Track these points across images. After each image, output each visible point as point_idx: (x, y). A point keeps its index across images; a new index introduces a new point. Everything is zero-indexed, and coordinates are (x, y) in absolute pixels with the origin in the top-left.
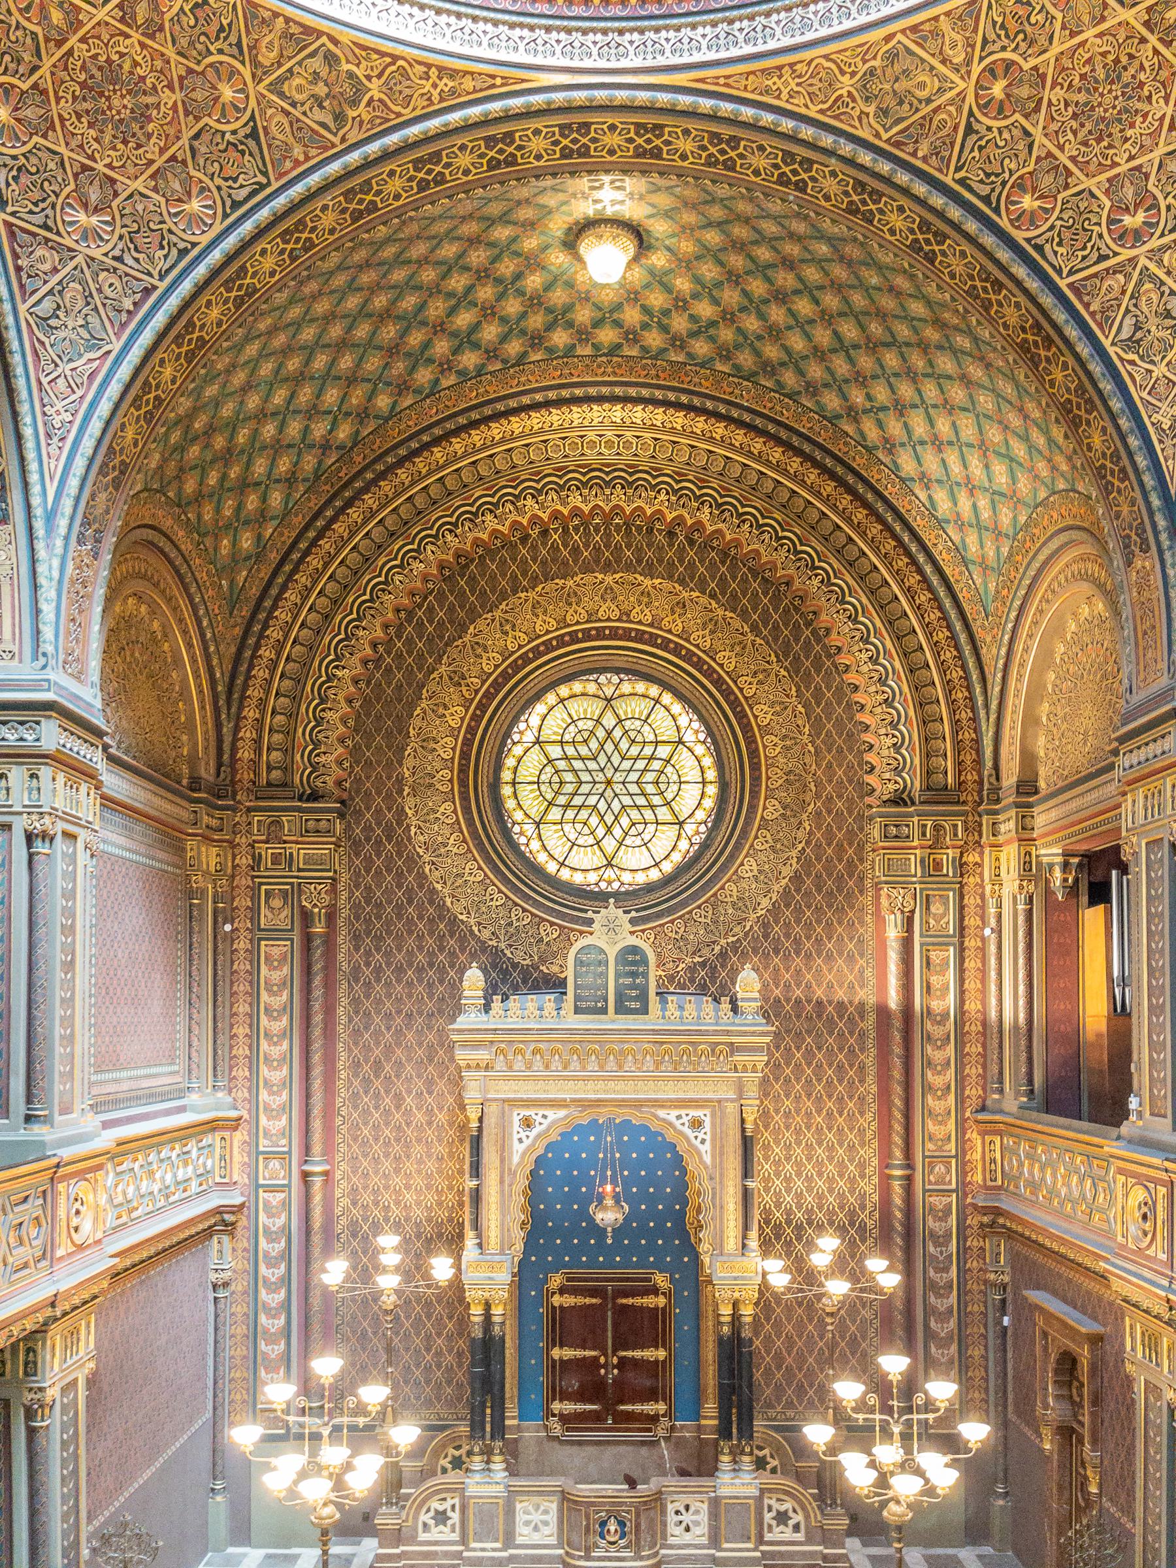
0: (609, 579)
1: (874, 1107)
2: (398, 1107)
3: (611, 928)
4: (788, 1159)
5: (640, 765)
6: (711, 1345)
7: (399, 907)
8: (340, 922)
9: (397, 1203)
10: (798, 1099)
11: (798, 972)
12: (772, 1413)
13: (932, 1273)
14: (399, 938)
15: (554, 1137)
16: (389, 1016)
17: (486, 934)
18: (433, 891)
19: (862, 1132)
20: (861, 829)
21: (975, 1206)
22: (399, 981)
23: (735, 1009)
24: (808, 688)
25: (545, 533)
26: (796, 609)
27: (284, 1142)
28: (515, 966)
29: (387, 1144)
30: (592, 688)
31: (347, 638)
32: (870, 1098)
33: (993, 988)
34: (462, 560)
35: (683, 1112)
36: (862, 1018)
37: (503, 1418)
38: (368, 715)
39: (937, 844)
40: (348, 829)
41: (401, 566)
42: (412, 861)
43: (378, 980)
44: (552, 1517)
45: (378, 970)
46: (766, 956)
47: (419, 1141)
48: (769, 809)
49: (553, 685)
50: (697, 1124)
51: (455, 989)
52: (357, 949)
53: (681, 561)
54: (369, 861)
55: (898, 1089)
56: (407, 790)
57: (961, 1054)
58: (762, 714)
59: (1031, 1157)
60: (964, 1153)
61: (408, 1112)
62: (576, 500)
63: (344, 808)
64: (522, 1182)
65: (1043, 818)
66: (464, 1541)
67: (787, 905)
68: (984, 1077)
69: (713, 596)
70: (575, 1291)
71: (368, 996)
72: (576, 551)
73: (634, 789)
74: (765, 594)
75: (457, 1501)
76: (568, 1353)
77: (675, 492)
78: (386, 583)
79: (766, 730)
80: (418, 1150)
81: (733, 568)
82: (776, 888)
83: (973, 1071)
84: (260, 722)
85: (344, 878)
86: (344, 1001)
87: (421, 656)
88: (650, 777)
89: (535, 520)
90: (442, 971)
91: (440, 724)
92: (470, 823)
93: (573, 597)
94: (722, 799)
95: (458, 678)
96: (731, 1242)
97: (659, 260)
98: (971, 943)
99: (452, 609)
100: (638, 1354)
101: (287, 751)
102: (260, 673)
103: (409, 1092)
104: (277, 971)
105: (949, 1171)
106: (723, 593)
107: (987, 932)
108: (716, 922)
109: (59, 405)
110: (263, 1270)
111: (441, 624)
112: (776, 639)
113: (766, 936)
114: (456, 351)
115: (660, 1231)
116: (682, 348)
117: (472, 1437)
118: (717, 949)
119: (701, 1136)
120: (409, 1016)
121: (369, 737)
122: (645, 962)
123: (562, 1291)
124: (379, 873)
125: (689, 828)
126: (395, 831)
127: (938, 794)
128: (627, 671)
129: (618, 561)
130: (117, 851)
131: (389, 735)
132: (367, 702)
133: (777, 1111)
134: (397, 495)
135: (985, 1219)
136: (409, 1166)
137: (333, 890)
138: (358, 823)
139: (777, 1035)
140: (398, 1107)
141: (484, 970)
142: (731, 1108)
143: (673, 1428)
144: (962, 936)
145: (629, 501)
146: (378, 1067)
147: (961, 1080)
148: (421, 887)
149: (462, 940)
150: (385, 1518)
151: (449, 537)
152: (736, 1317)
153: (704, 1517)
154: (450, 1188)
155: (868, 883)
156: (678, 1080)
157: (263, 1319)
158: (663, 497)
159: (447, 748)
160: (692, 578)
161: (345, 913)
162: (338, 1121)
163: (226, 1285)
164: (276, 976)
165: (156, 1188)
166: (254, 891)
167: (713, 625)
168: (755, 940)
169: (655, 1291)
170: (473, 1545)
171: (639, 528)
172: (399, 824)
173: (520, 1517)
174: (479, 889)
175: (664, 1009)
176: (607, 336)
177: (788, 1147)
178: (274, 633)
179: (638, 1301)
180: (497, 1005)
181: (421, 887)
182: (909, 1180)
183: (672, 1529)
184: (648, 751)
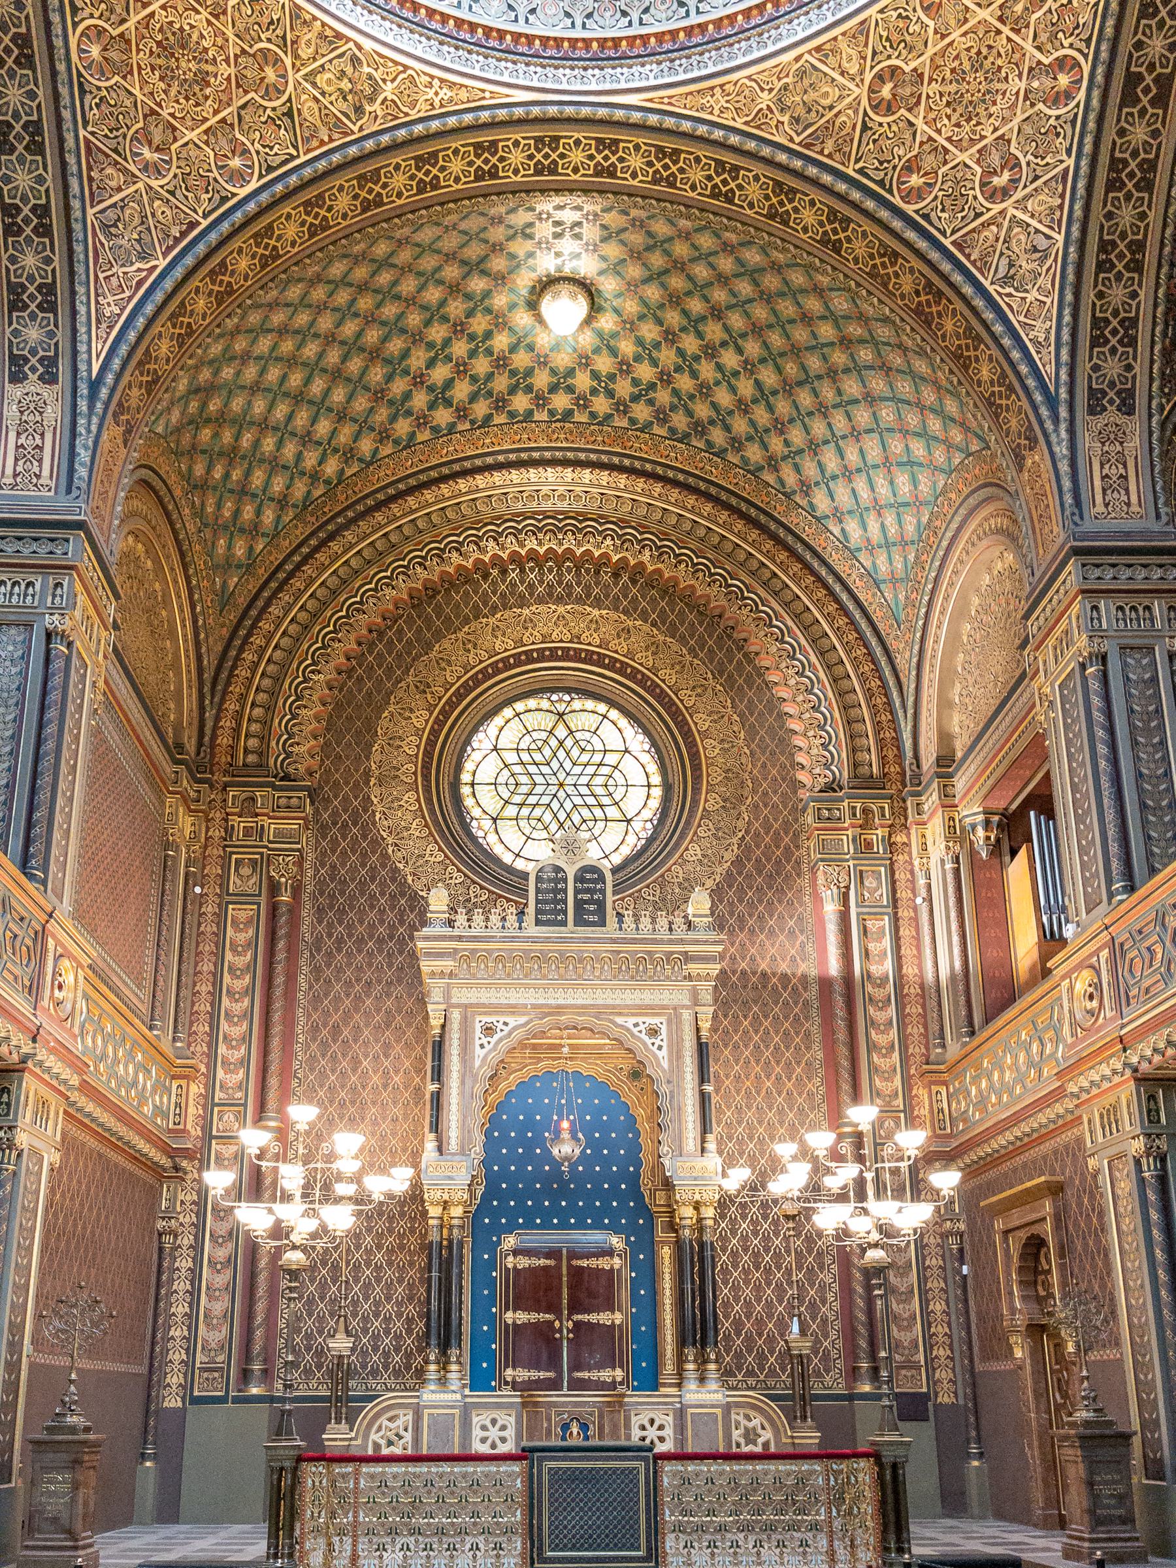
0: (561, 609)
1: (821, 1072)
2: (354, 1070)
5: (590, 770)
8: (305, 897)
11: (742, 945)
14: (362, 912)
16: (348, 984)
22: (360, 951)
25: (504, 572)
26: (730, 637)
30: (545, 704)
33: (928, 952)
35: (640, 1020)
39: (866, 825)
40: (317, 812)
42: (377, 843)
43: (339, 950)
45: (340, 941)
47: (374, 1103)
48: (710, 801)
49: (509, 702)
50: (653, 1032)
54: (335, 843)
55: (843, 1051)
58: (700, 722)
60: (912, 1109)
61: (365, 1074)
63: (313, 793)
65: (960, 783)
67: (730, 886)
68: (926, 1036)
69: (654, 624)
71: (328, 965)
72: (531, 586)
73: (584, 790)
79: (705, 735)
81: (672, 603)
83: (915, 1030)
84: (238, 716)
85: (311, 857)
87: (390, 669)
91: (406, 729)
92: (432, 811)
95: (423, 687)
97: (607, 322)
98: (904, 913)
101: (264, 738)
102: (242, 672)
104: (242, 932)
107: (919, 901)
111: (409, 642)
116: (625, 412)
120: (369, 984)
124: (344, 853)
125: (637, 825)
126: (361, 816)
127: (864, 782)
128: (577, 691)
129: (569, 595)
131: (358, 733)
132: (339, 706)
140: (354, 1070)
144: (895, 907)
146: (336, 1031)
148: (384, 866)
155: (805, 867)
159: (412, 746)
161: (310, 888)
162: (294, 1083)
164: (242, 938)
166: (225, 861)
167: (655, 648)
171: (588, 571)
172: (365, 811)
177: (739, 1110)
178: (257, 640)
181: (384, 866)
184: (597, 758)
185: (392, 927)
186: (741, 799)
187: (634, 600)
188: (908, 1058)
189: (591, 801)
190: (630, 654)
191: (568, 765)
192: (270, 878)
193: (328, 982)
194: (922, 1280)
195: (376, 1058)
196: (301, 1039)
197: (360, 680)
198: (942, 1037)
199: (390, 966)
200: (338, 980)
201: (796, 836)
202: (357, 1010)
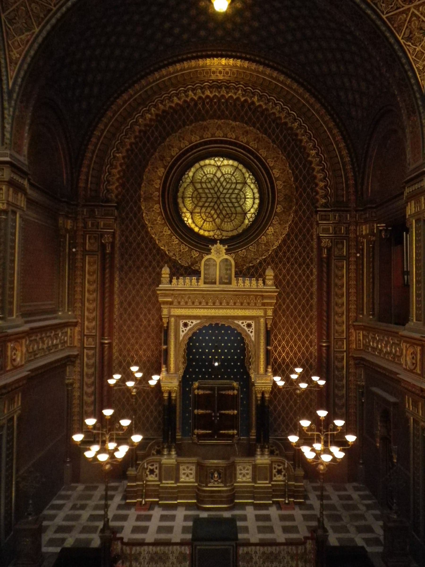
0: (219, 122)
3: (218, 252)
4: (284, 339)
6: (254, 409)
7: (139, 245)
8: (116, 249)
9: (137, 355)
10: (288, 317)
12: (276, 434)
13: (336, 382)
15: (195, 330)
16: (134, 285)
17: (171, 254)
18: (152, 238)
19: (311, 329)
20: (312, 216)
21: (352, 356)
23: (264, 283)
25: (196, 104)
27: (94, 331)
28: (182, 266)
29: (133, 333)
31: (121, 142)
34: (165, 114)
36: (312, 287)
37: (175, 436)
42: (144, 226)
44: (194, 472)
45: (130, 267)
46: (276, 264)
47: (145, 331)
48: (279, 209)
51: (159, 274)
52: (122, 259)
56: (142, 200)
57: (348, 301)
58: (276, 173)
59: (374, 339)
60: (349, 337)
61: (141, 321)
62: (208, 93)
64: (184, 347)
66: (160, 480)
69: (258, 129)
70: (204, 389)
72: (207, 112)
75: (158, 465)
76: (201, 412)
77: (245, 91)
79: (277, 179)
80: (144, 335)
83: (353, 307)
86: (117, 279)
88: (234, 196)
89: (192, 99)
90: (154, 268)
93: (205, 128)
94: (260, 205)
95: (162, 158)
96: (262, 370)
100: (227, 412)
103: (141, 313)
105: (343, 344)
108: (258, 251)
109: (15, 51)
110: (85, 379)
113: (277, 256)
115: (235, 366)
117: (163, 442)
118: (258, 261)
119: (251, 330)
120: (142, 285)
122: (231, 265)
123: (198, 388)
130: (32, 219)
133: (280, 322)
134: (141, 90)
135: (357, 362)
136: (141, 341)
137: (114, 237)
139: (280, 293)
140: (137, 319)
141: (170, 268)
142: (262, 320)
143: (240, 439)
145: (227, 93)
146: (130, 304)
147: (348, 310)
148: (147, 236)
149: (162, 256)
150: (131, 472)
151: (160, 105)
152: (263, 397)
153: (250, 472)
154: (157, 349)
155: (315, 237)
156: (242, 309)
157: (85, 398)
158: (240, 92)
159: (158, 184)
161: (118, 245)
162: (115, 324)
163: (72, 384)
165: (45, 346)
167: (258, 140)
168: (272, 258)
169: (233, 389)
170: (164, 482)
172: (139, 212)
173: (182, 472)
175: (237, 283)
176: (220, 33)
179: (227, 392)
180: (174, 281)
182: (328, 347)
183: (238, 476)
185: (150, 262)
186: (291, 208)
188: (349, 319)
189: (230, 205)
191: (221, 189)
192: (102, 243)
195: (145, 315)
196: (117, 306)
199: (150, 277)
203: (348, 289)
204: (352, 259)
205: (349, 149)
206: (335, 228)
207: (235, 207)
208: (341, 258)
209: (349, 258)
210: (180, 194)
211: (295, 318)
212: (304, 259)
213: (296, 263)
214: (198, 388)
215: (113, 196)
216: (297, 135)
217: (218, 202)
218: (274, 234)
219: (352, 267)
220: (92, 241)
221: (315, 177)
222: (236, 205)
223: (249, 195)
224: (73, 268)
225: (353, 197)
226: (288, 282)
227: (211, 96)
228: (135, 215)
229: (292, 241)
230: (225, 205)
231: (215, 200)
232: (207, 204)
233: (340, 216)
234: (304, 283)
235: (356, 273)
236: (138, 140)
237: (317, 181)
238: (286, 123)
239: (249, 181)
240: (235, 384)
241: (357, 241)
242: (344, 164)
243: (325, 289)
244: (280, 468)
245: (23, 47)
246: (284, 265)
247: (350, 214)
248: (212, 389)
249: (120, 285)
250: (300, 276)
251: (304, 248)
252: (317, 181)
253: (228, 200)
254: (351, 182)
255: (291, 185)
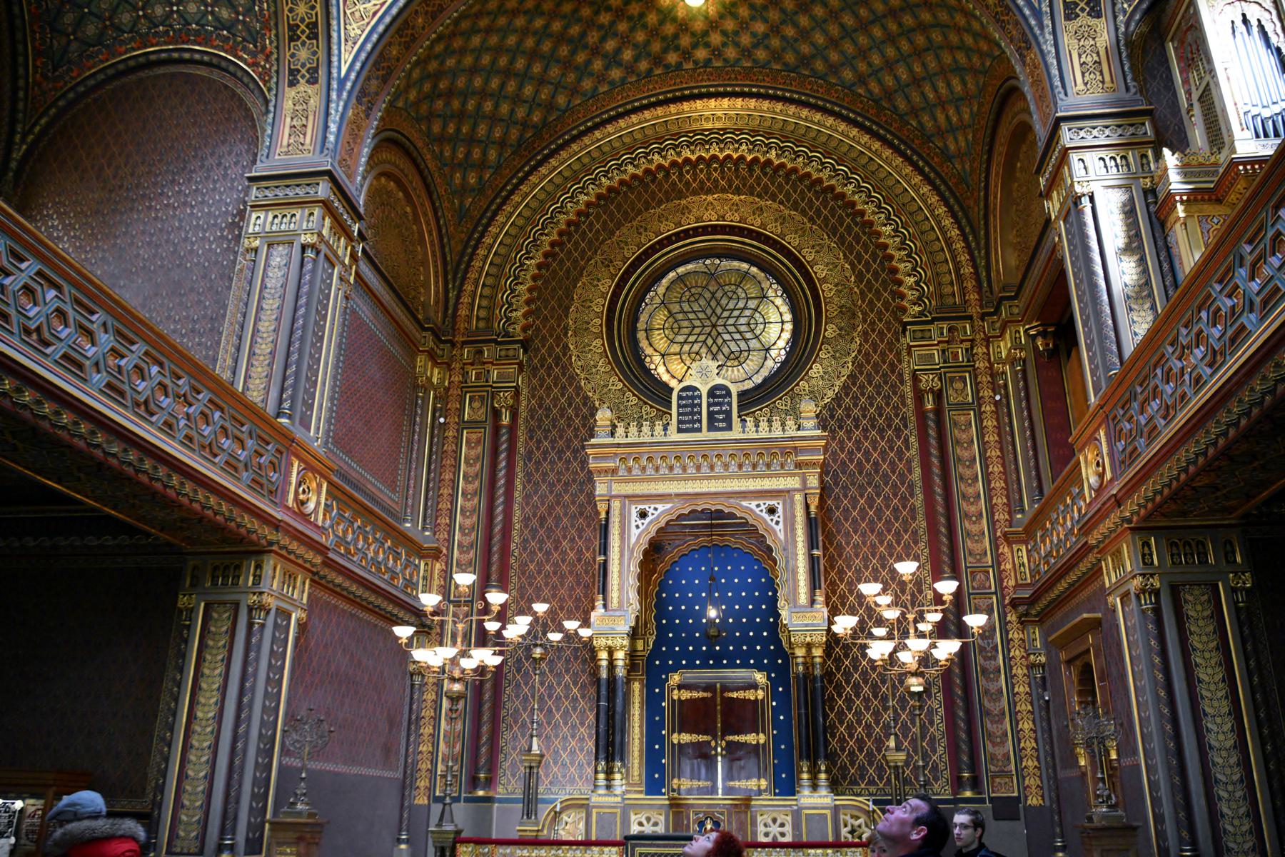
0: (710, 198)
1: (925, 538)
2: (556, 548)
7: (562, 410)
8: (520, 421)
14: (561, 431)
18: (587, 398)
20: (898, 340)
22: (560, 459)
24: (851, 253)
25: (667, 175)
32: (921, 532)
38: (546, 289)
40: (530, 359)
41: (572, 197)
42: (572, 378)
43: (545, 459)
45: (545, 453)
48: (830, 331)
52: (531, 438)
53: (759, 185)
54: (542, 381)
58: (819, 271)
60: (999, 564)
61: (564, 553)
62: (687, 153)
63: (525, 345)
67: (847, 395)
69: (781, 203)
72: (688, 184)
74: (817, 199)
77: (752, 143)
78: (561, 207)
79: (824, 280)
80: (570, 580)
82: (838, 383)
83: (1000, 500)
85: (524, 392)
86: (520, 475)
87: (583, 252)
89: (660, 167)
91: (595, 294)
93: (685, 210)
99: (605, 222)
104: (470, 450)
105: (988, 579)
106: (788, 201)
111: (598, 231)
112: (826, 226)
113: (832, 417)
114: (607, 68)
115: (758, 639)
121: (546, 302)
123: (680, 687)
125: (773, 353)
126: (561, 360)
129: (716, 187)
131: (560, 299)
132: (546, 282)
138: (536, 356)
145: (721, 150)
146: (542, 520)
147: (991, 509)
148: (578, 395)
151: (603, 180)
155: (907, 377)
158: (744, 147)
159: (600, 305)
160: (766, 193)
162: (512, 560)
167: (783, 220)
169: (754, 686)
171: (729, 169)
172: (564, 355)
174: (618, 394)
181: (578, 395)
186: (854, 327)
187: (766, 186)
188: (994, 523)
190: (763, 226)
192: (493, 408)
193: (537, 484)
194: (1012, 704)
196: (517, 526)
197: (562, 261)
198: (1022, 505)
200: (544, 481)
201: (898, 354)
202: (558, 503)
203: (985, 466)
204: (988, 408)
205: (954, 216)
206: (943, 351)
207: (746, 340)
208: (963, 407)
209: (980, 406)
210: (641, 325)
211: (880, 535)
212: (889, 419)
213: (873, 427)
214: (680, 687)
215: (518, 328)
216: (853, 204)
217: (714, 333)
218: (825, 375)
219: (990, 423)
220: (476, 405)
221: (895, 271)
222: (748, 335)
223: (773, 316)
224: (438, 455)
225: (973, 297)
226: (860, 466)
227: (693, 158)
228: (557, 360)
229: (862, 387)
230: (727, 337)
231: (708, 330)
232: (692, 339)
233: (950, 330)
234: (893, 466)
235: (999, 435)
236: (565, 238)
237: (899, 276)
238: (832, 188)
239: (770, 293)
240: (760, 677)
241: (991, 375)
242: (949, 243)
243: (936, 471)
244: (857, 823)
245: (367, 20)
246: (849, 432)
247: (972, 327)
248: (709, 688)
249: (524, 487)
250: (883, 454)
251: (887, 398)
252: (899, 276)
253: (731, 329)
254: (967, 270)
255: (852, 289)
